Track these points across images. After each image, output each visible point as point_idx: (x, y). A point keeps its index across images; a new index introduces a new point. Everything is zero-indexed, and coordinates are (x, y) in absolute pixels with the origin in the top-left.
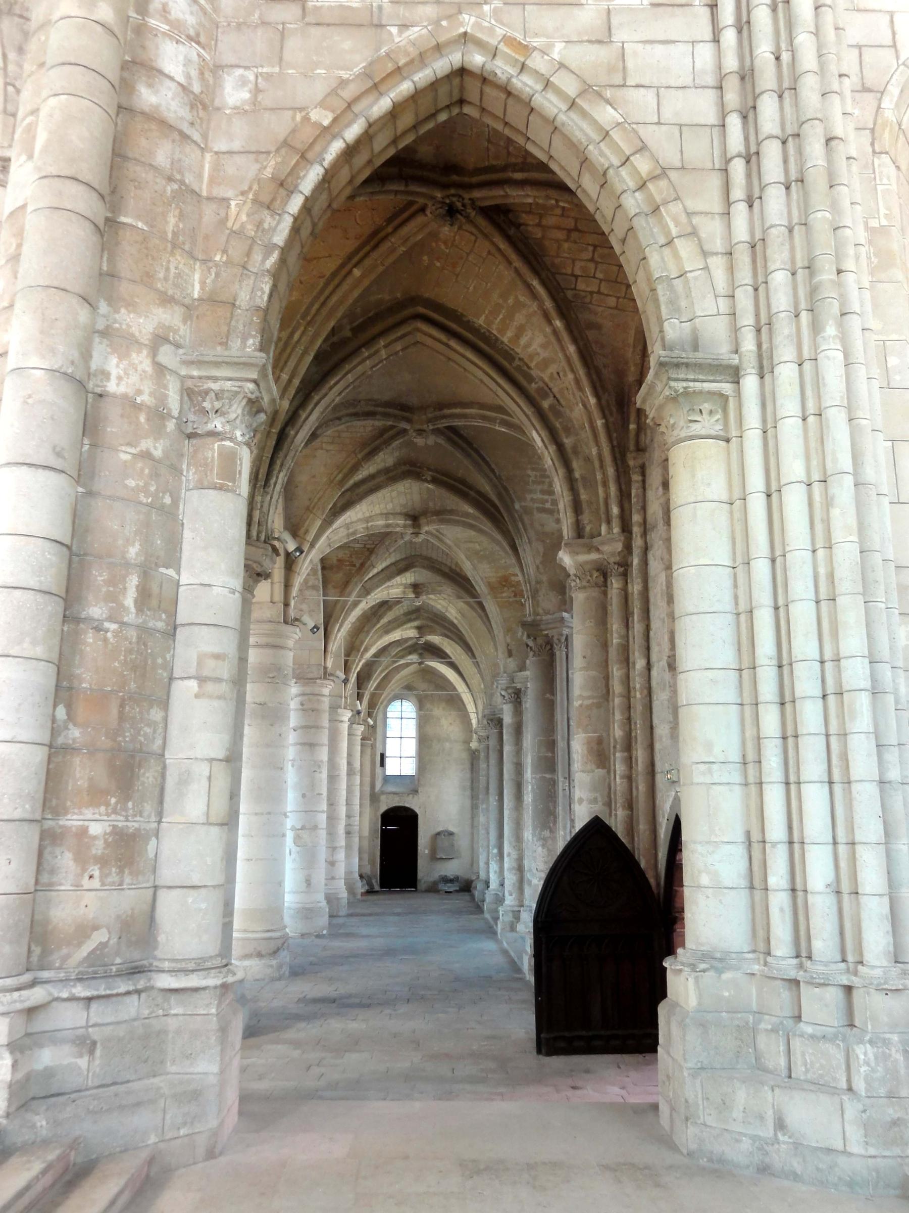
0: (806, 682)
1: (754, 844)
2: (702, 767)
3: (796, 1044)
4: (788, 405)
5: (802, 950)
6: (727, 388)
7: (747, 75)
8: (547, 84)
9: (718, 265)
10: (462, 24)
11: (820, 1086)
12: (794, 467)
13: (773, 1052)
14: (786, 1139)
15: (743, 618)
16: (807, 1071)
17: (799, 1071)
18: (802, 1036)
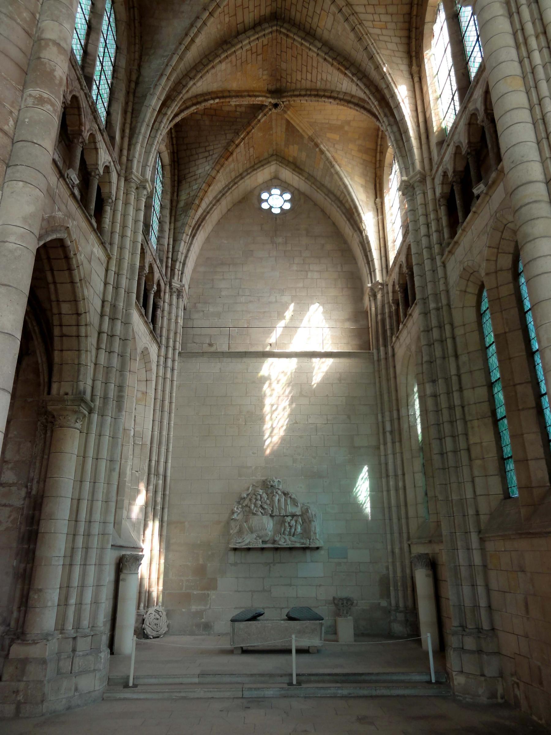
0: (96, 529)
1: (65, 589)
2: (57, 558)
3: (76, 660)
4: (107, 431)
5: (77, 626)
6: (86, 413)
7: (114, 307)
8: (78, 267)
9: (93, 366)
10: (69, 223)
11: (84, 672)
12: (104, 454)
13: (66, 665)
14: (78, 694)
15: (75, 502)
16: (79, 668)
17: (76, 669)
18: (79, 656)
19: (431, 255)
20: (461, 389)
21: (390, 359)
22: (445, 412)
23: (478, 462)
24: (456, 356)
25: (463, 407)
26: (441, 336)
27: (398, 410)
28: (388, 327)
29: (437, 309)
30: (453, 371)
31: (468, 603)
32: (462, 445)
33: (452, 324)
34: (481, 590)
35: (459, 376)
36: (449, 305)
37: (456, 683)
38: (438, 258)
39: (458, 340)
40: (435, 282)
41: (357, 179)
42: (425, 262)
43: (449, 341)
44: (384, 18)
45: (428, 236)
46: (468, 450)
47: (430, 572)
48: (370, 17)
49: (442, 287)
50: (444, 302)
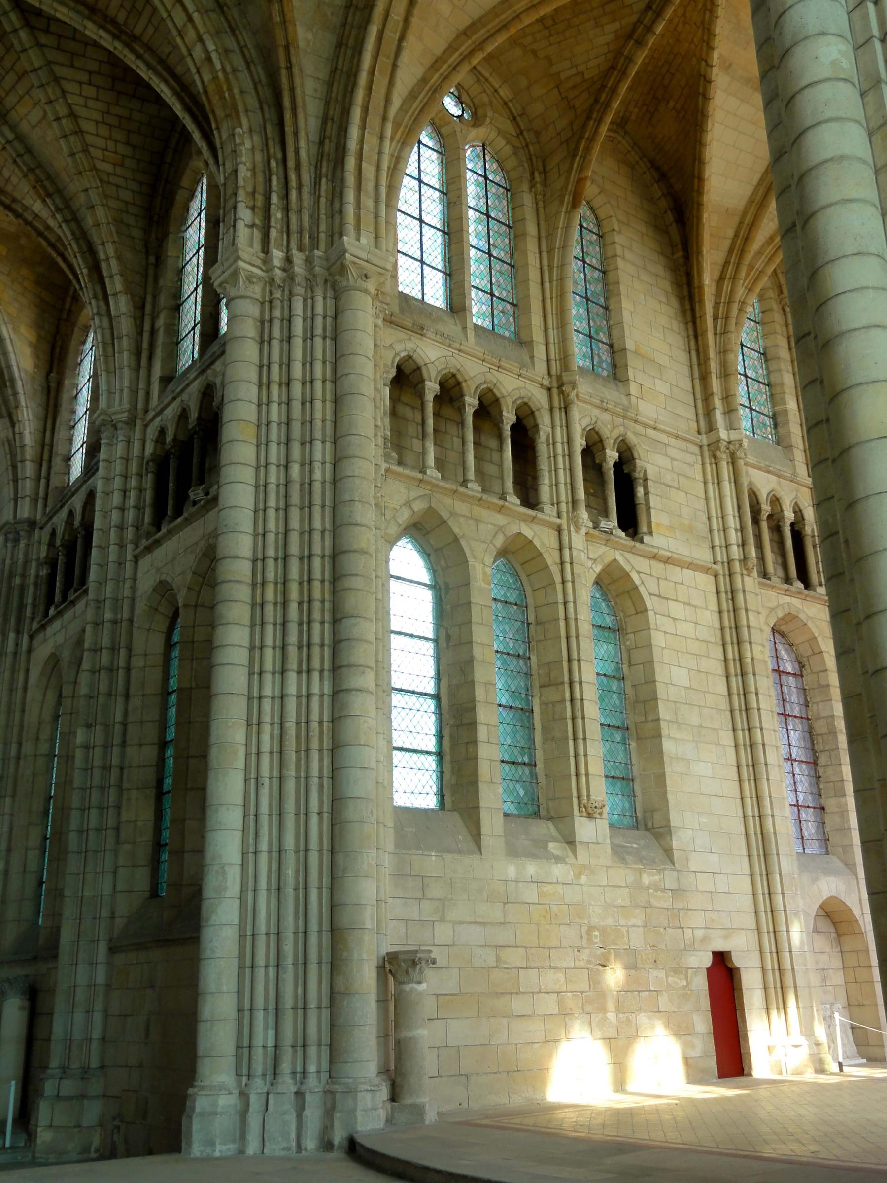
19: (121, 539)
20: (124, 744)
21: (23, 657)
22: (97, 773)
23: (127, 847)
24: (127, 696)
25: (122, 769)
26: (112, 663)
27: (20, 744)
28: (29, 600)
29: (115, 622)
30: (119, 717)
31: (77, 1036)
32: (111, 822)
33: (129, 649)
34: (97, 1017)
35: (125, 724)
36: (131, 621)
37: (39, 1141)
38: (130, 547)
39: (133, 673)
40: (118, 581)
41: (23, 330)
42: (112, 547)
43: (121, 673)
44: (121, 148)
45: (122, 509)
46: (117, 829)
47: (26, 1003)
48: (100, 142)
49: (127, 593)
50: (126, 615)
